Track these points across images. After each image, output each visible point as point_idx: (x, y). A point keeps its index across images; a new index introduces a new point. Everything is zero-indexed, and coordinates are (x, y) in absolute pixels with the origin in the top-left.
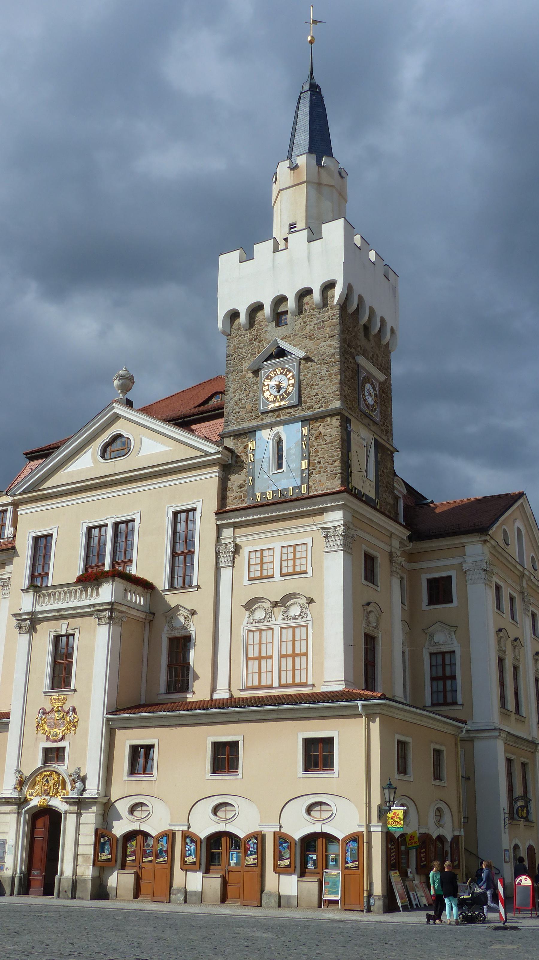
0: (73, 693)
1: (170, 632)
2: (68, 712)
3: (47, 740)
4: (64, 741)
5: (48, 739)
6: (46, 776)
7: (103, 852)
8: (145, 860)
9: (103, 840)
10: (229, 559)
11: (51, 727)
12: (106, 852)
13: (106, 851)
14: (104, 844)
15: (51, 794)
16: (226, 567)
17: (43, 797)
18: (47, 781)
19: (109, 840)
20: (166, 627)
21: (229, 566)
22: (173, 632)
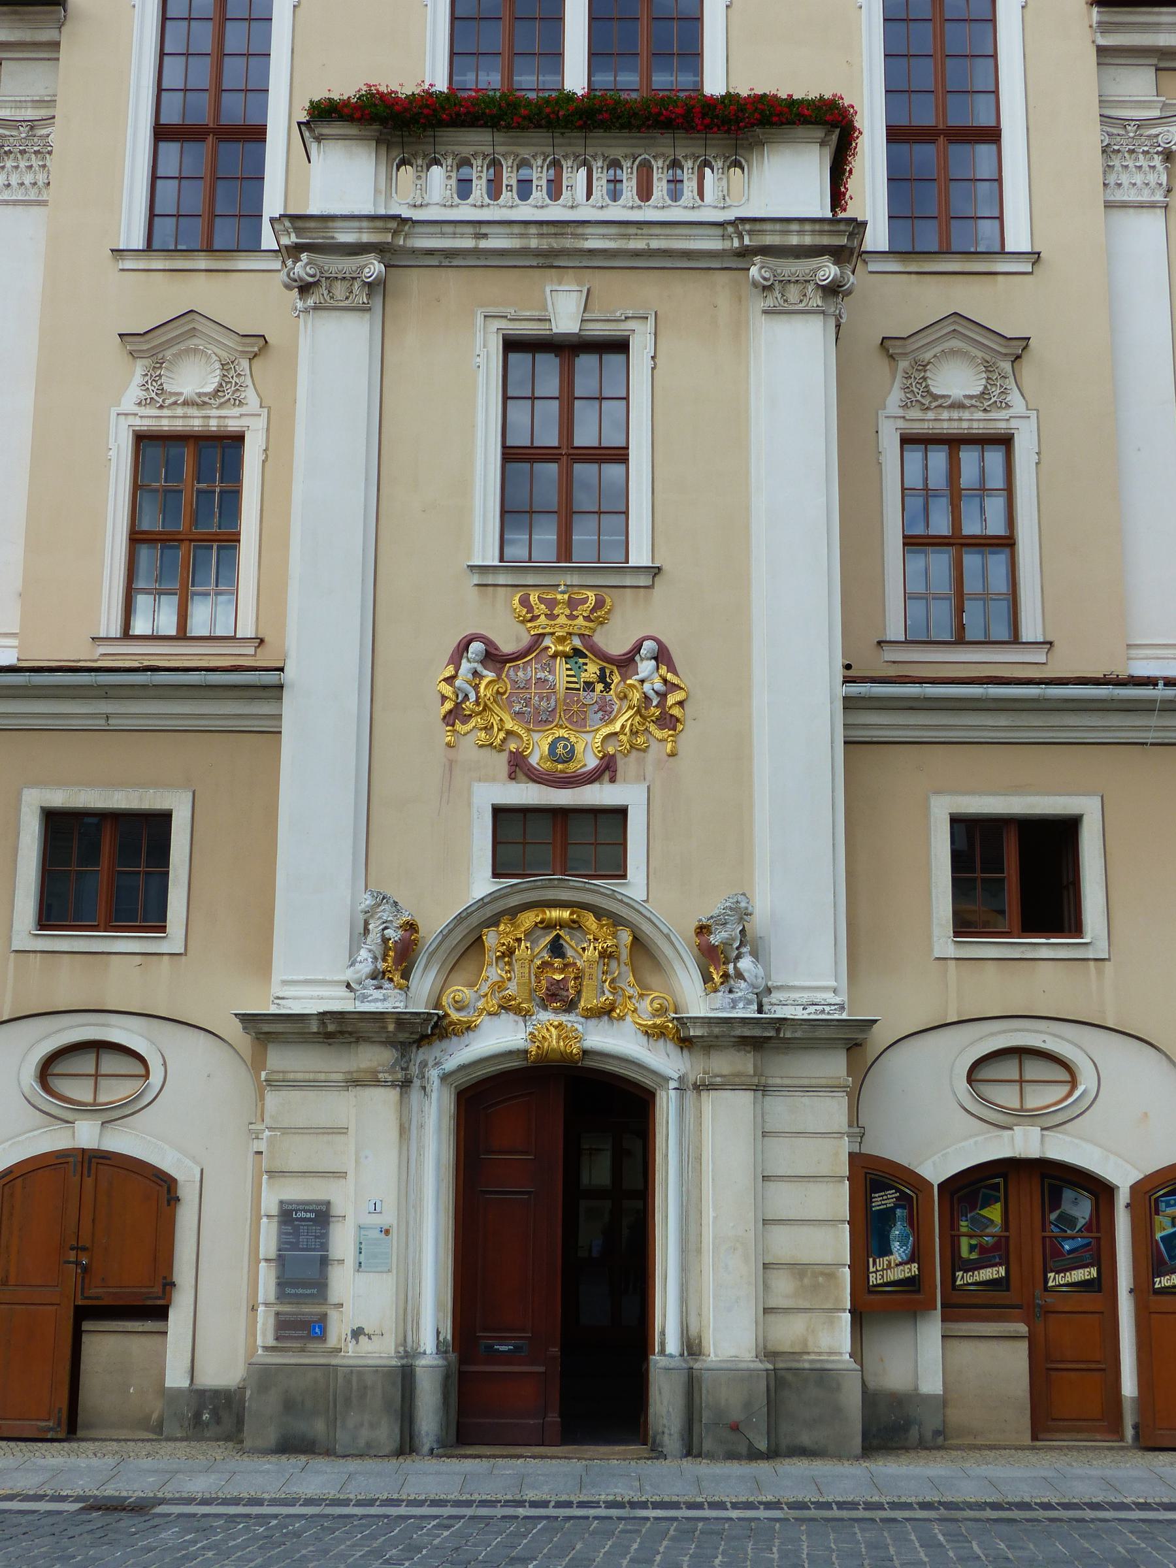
0: (644, 580)
1: (915, 413)
2: (626, 663)
3: (512, 777)
4: (613, 780)
5: (519, 767)
6: (549, 926)
7: (886, 1251)
8: (1054, 1279)
9: (883, 1200)
10: (1152, 178)
11: (541, 720)
12: (899, 1252)
13: (896, 1246)
14: (885, 1219)
15: (589, 1000)
16: (1141, 206)
17: (545, 1016)
18: (556, 948)
19: (904, 1200)
20: (896, 396)
21: (1152, 206)
22: (930, 415)
